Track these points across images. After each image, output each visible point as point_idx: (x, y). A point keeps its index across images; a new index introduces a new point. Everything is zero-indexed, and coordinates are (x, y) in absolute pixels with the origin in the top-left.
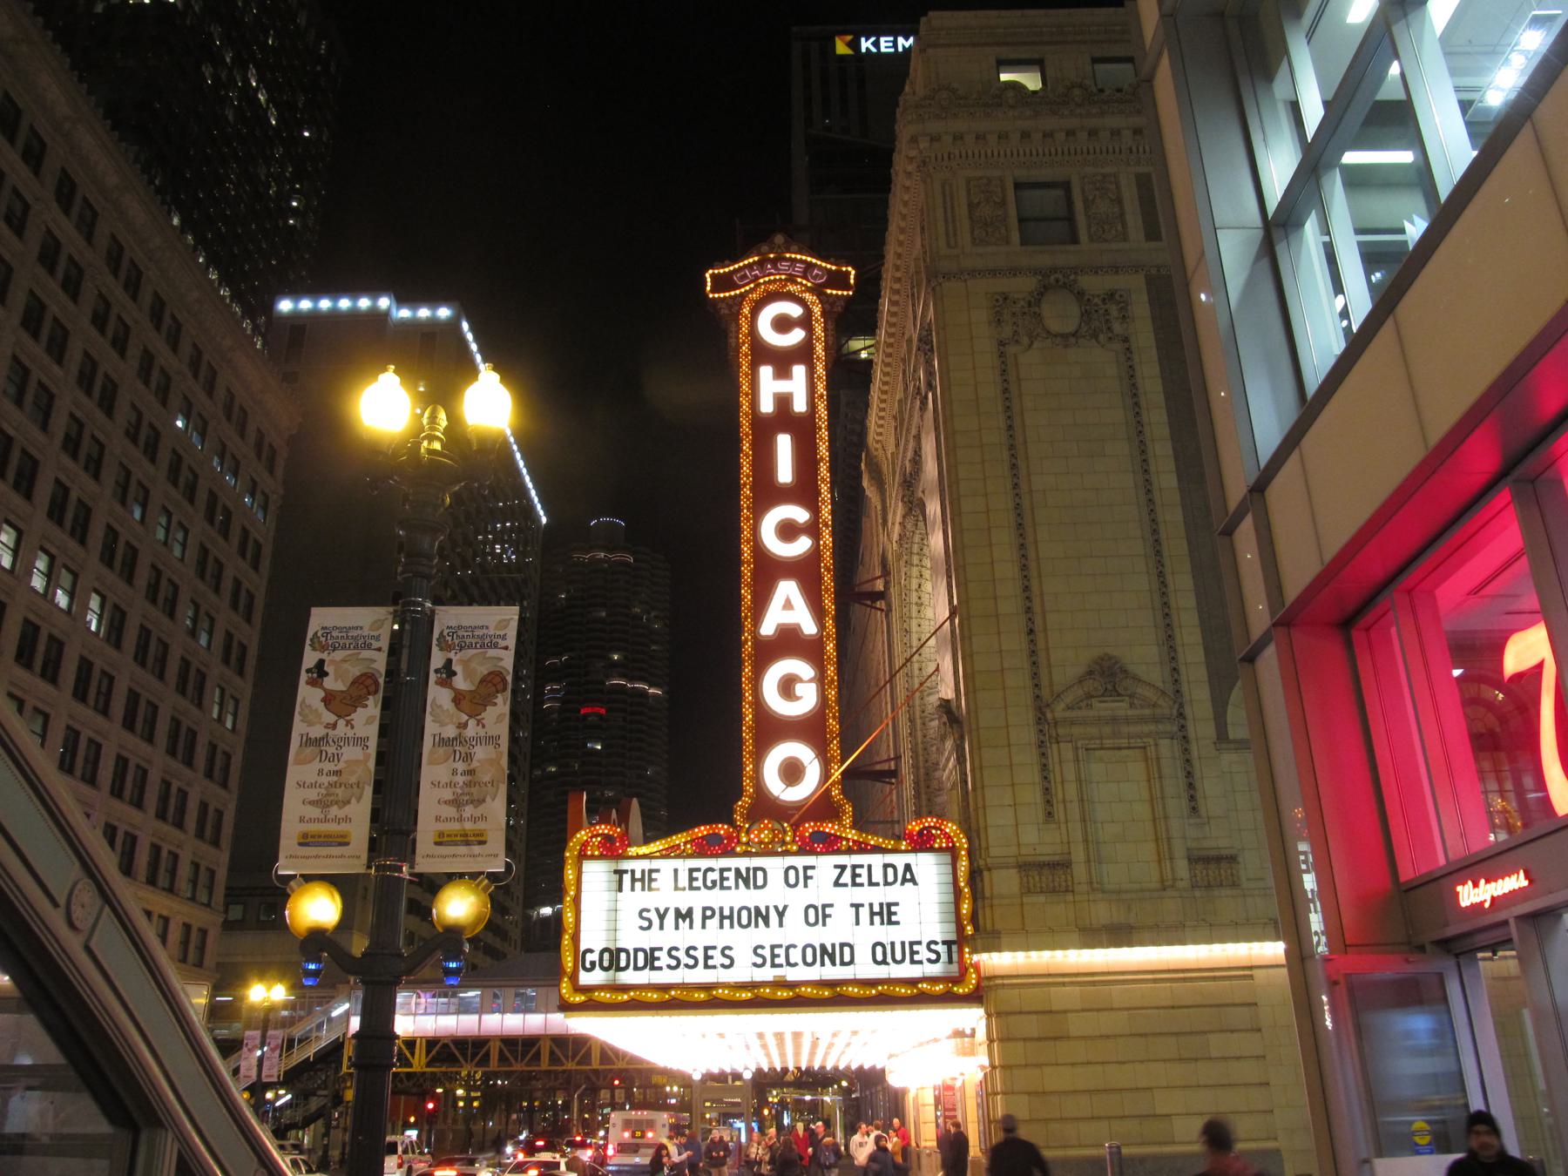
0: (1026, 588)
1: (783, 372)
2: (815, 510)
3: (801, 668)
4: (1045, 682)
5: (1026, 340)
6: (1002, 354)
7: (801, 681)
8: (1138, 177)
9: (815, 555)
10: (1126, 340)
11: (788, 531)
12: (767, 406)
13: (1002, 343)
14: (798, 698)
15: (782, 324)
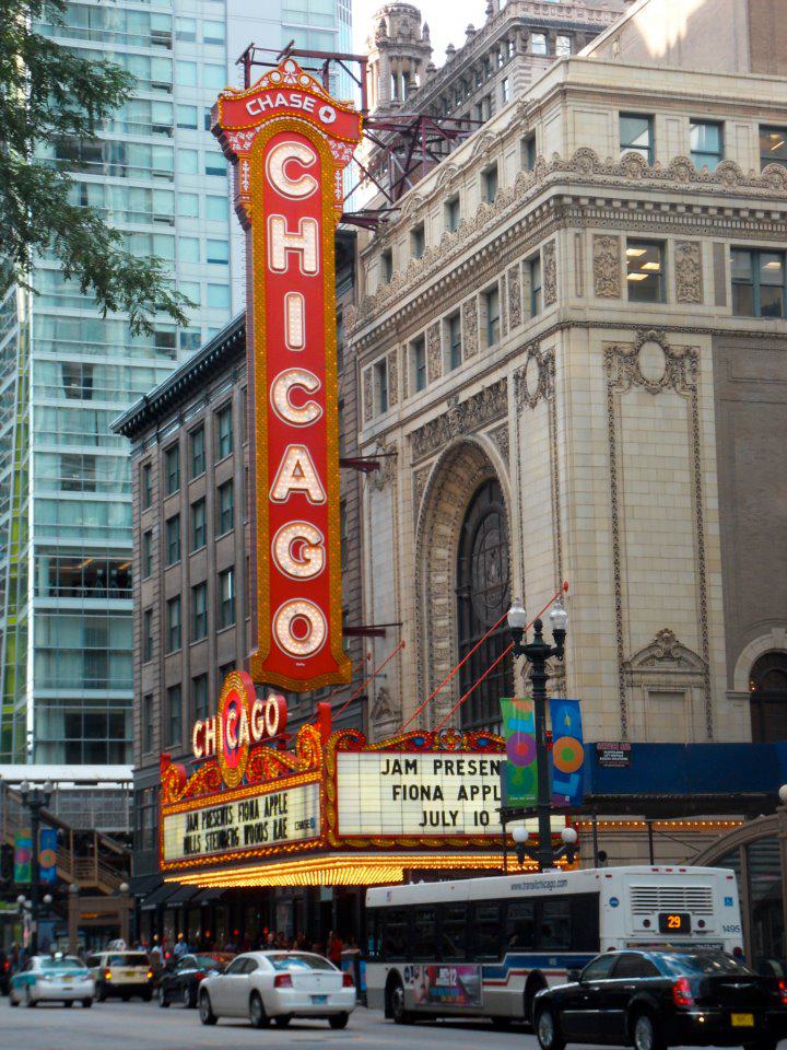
0: (617, 578)
1: (293, 227)
2: (322, 377)
3: (309, 532)
4: (626, 643)
5: (626, 383)
6: (610, 395)
7: (312, 546)
8: (716, 245)
9: (319, 426)
10: (694, 390)
11: (298, 397)
12: (279, 261)
13: (610, 386)
14: (308, 561)
15: (294, 169)
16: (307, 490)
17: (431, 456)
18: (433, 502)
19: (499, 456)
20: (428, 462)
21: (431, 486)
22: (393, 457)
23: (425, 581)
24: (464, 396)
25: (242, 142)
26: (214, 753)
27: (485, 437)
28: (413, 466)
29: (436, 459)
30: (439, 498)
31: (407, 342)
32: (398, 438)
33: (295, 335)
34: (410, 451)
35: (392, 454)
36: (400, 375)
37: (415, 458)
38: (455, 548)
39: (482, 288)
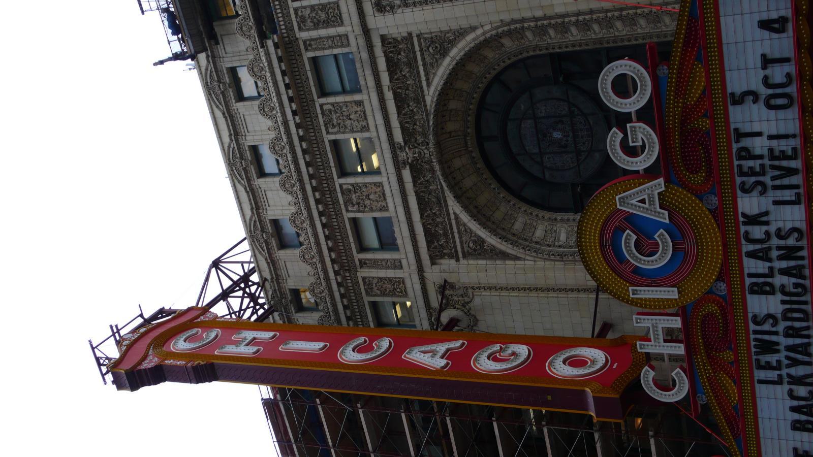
14: (514, 354)
16: (448, 350)
17: (448, 214)
18: (489, 224)
19: (447, 60)
20: (452, 217)
21: (473, 216)
22: (447, 292)
23: (562, 249)
24: (398, 137)
25: (151, 361)
26: (676, 323)
28: (458, 260)
29: (454, 206)
30: (489, 219)
31: (358, 257)
32: (434, 275)
33: (314, 346)
34: (447, 264)
35: (445, 287)
36: (382, 273)
37: (451, 256)
38: (536, 211)
39: (315, 97)
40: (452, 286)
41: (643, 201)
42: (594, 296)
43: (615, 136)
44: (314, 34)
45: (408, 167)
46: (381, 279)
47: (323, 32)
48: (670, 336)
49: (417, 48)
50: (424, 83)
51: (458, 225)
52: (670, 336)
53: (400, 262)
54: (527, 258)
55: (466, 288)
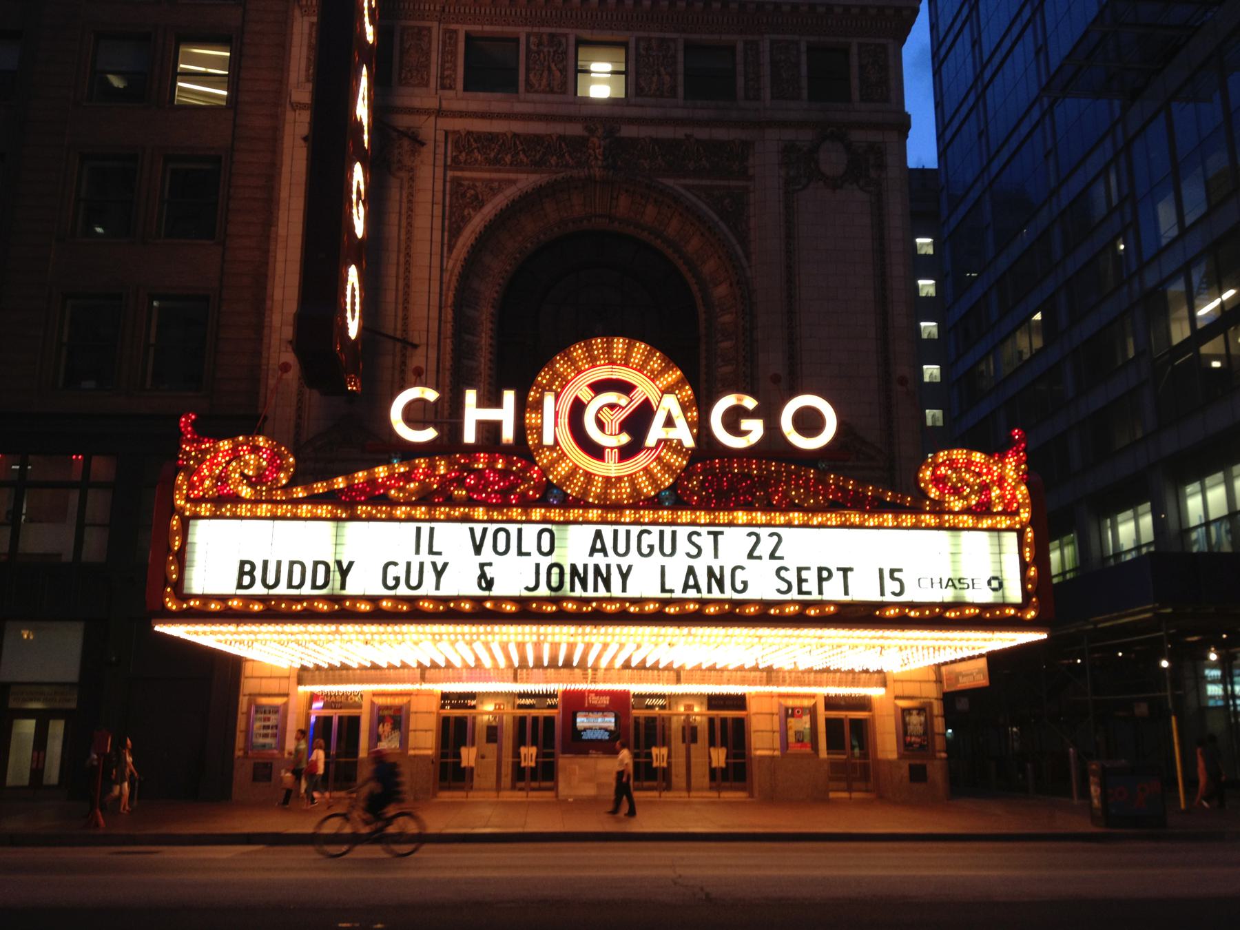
17: (517, 172)
19: (716, 218)
20: (512, 176)
27: (683, 191)
35: (417, 141)
37: (455, 159)
40: (413, 152)
41: (669, 422)
42: (399, 334)
43: (750, 403)
44: (766, 58)
45: (586, 134)
46: (428, 54)
47: (766, 70)
48: (490, 430)
49: (733, 183)
50: (689, 182)
51: (500, 181)
52: (490, 430)
53: (451, 88)
54: (451, 263)
55: (412, 170)
